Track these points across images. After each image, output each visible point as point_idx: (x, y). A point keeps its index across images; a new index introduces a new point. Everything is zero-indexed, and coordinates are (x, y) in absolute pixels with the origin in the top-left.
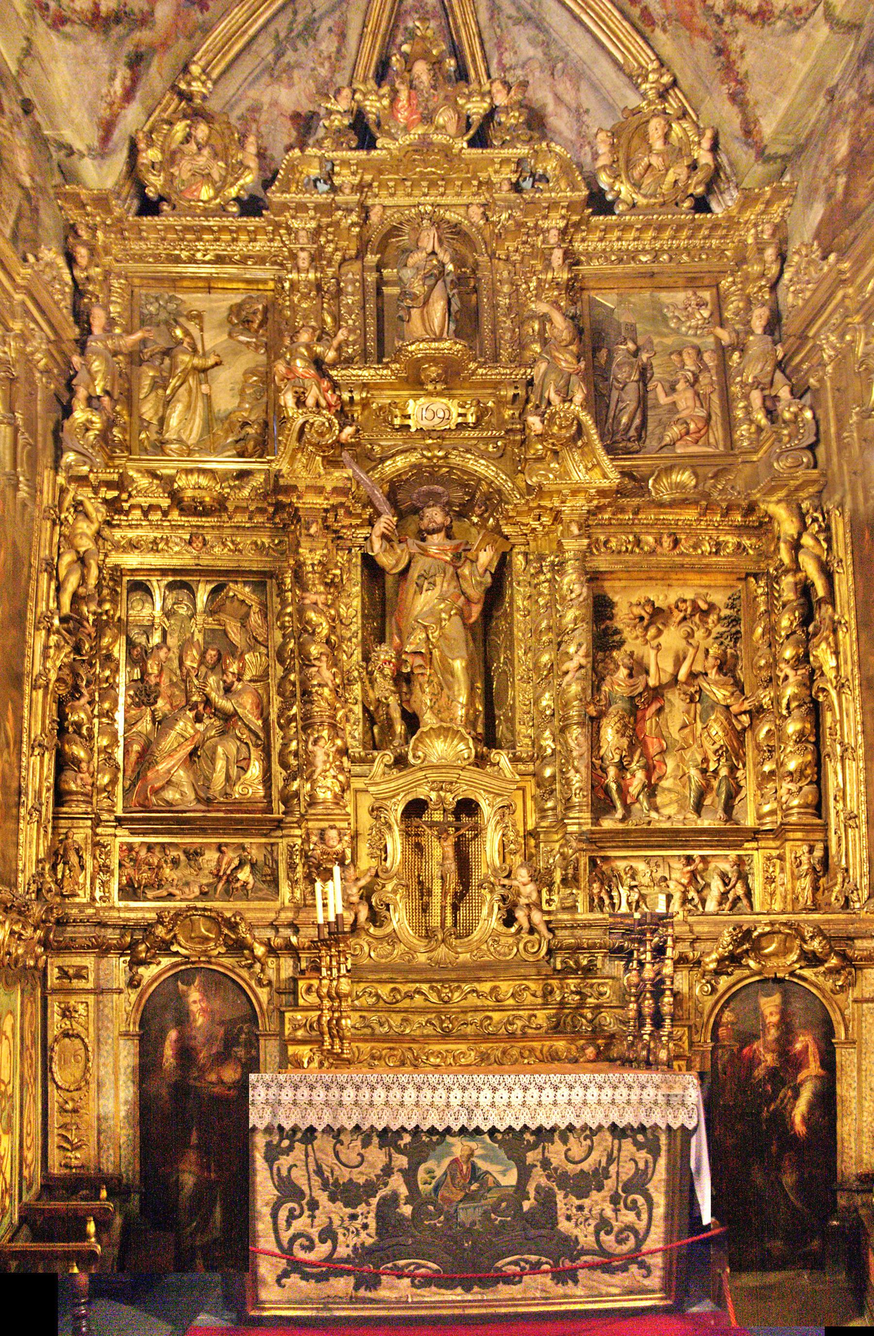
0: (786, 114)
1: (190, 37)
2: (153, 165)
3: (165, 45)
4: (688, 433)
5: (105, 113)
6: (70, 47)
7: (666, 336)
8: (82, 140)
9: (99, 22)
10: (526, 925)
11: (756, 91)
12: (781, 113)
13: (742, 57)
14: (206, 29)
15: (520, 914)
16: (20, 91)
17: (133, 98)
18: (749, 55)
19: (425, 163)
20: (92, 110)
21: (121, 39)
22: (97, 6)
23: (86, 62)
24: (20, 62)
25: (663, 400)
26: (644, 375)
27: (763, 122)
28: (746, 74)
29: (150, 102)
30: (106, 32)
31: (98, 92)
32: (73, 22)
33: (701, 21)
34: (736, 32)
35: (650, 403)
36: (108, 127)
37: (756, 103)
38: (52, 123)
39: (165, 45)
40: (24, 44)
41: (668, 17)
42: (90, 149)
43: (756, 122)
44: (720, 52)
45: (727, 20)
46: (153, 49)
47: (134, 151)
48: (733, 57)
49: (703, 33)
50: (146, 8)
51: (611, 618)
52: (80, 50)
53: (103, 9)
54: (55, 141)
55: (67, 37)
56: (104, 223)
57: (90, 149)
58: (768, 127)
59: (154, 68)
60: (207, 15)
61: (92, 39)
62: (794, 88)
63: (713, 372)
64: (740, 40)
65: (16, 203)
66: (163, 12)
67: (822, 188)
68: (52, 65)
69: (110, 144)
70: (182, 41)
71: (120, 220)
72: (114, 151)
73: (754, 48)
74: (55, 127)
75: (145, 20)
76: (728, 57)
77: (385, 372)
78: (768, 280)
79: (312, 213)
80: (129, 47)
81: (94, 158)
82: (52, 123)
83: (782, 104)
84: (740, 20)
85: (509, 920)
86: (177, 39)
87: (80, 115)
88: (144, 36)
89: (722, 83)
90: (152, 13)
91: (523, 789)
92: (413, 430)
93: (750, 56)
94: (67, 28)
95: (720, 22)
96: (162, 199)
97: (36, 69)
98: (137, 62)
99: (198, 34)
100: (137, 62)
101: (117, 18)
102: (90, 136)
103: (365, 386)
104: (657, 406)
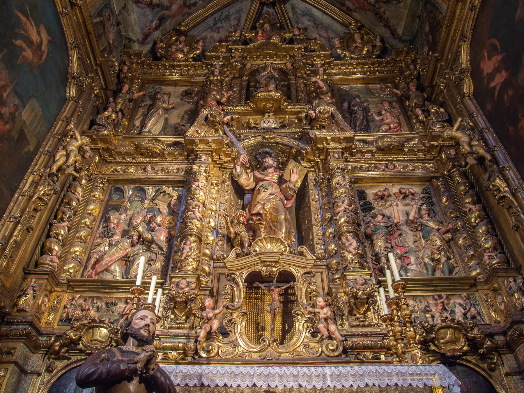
0: (405, 26)
1: (183, 16)
2: (162, 47)
3: (173, 16)
4: (390, 128)
5: (146, 30)
6: (139, 10)
7: (374, 98)
8: (136, 36)
9: (151, 5)
10: (326, 333)
11: (392, 22)
12: (403, 26)
13: (385, 14)
14: (189, 14)
15: (321, 326)
16: (117, 19)
17: (159, 29)
18: (387, 13)
19: (268, 49)
20: (142, 29)
21: (158, 12)
22: (152, 1)
23: (144, 15)
24: (120, 11)
25: (377, 118)
26: (366, 110)
27: (398, 30)
28: (388, 18)
29: (164, 32)
30: (153, 9)
31: (146, 24)
32: (142, 3)
33: (367, 7)
34: (381, 7)
35: (370, 120)
36: (146, 36)
37: (394, 26)
38: (126, 30)
39: (173, 16)
40: (123, 6)
41: (356, 8)
42: (138, 40)
43: (395, 30)
44: (376, 14)
45: (377, 5)
46: (169, 17)
47: (155, 43)
48: (381, 14)
49: (369, 10)
50: (169, 5)
51: (365, 199)
52: (142, 11)
53: (154, 2)
54: (125, 37)
55: (139, 7)
56: (137, 62)
57: (138, 40)
58: (400, 31)
59: (168, 22)
60: (190, 10)
61: (148, 9)
62: (405, 18)
63: (398, 108)
64: (382, 9)
65: (105, 46)
66: (174, 7)
67: (425, 42)
68: (132, 13)
69: (146, 41)
70: (180, 16)
71: (144, 62)
72: (147, 43)
73: (388, 11)
74: (126, 32)
75: (168, 8)
76: (380, 15)
77: (247, 108)
78: (414, 76)
79: (221, 59)
80: (160, 14)
81: (139, 43)
82: (126, 30)
83: (403, 23)
84: (381, 4)
85: (314, 333)
86: (178, 15)
87: (137, 29)
88: (167, 12)
89: (380, 22)
90: (171, 7)
91: (321, 273)
92: (260, 128)
93: (387, 13)
94: (140, 5)
95: (374, 6)
96: (162, 57)
97: (125, 13)
98: (162, 19)
99: (186, 15)
100: (162, 19)
101: (158, 6)
102: (140, 37)
103: (239, 113)
104: (374, 120)
